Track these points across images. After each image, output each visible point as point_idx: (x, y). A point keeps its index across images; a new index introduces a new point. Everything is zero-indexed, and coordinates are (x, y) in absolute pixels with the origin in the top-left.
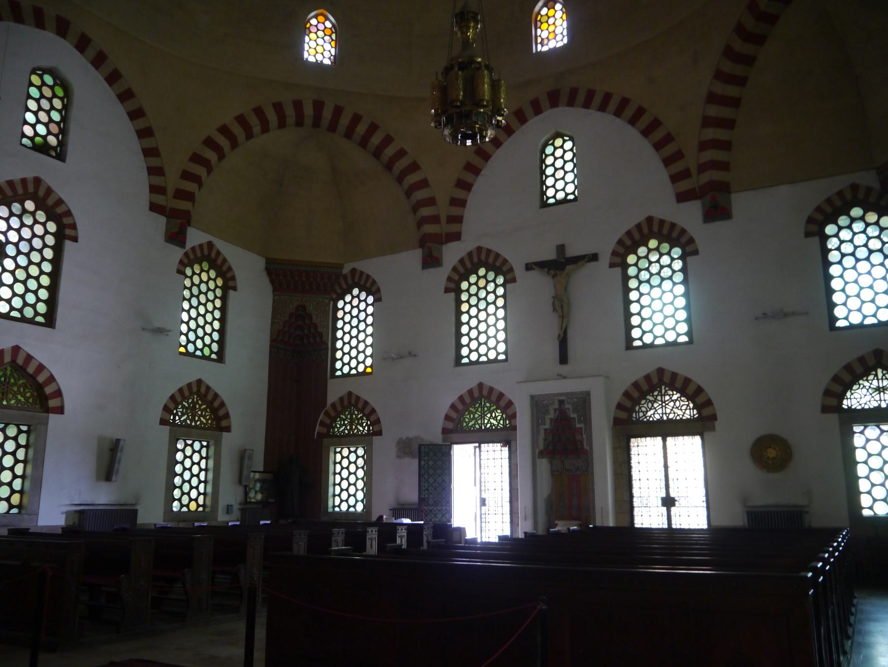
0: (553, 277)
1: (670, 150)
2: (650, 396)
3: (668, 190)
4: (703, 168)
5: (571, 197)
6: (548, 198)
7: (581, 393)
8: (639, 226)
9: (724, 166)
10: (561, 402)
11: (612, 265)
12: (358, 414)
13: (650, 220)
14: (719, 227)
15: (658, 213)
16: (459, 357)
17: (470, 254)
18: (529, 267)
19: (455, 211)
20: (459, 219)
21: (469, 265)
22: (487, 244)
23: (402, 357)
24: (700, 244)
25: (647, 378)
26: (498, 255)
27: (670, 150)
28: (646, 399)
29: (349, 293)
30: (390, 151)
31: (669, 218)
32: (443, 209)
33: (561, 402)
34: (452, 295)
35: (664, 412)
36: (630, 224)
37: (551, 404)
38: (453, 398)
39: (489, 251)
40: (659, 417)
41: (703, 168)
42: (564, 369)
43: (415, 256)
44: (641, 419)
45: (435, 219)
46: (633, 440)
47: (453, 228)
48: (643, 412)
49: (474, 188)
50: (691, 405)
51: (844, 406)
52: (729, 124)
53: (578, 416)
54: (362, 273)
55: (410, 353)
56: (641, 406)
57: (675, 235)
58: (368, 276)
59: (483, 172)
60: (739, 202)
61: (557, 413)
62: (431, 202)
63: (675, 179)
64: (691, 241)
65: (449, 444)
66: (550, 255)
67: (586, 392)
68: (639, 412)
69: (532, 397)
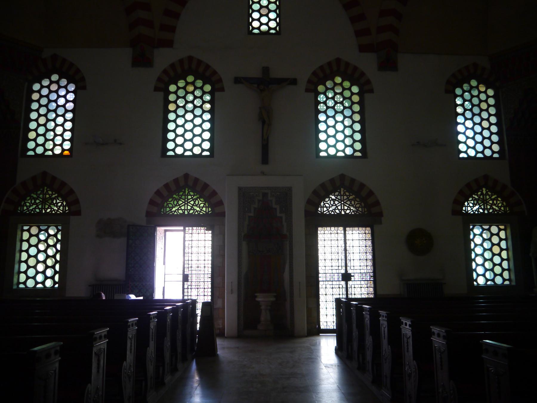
2: (332, 195)
6: (254, 28)
8: (329, 64)
10: (265, 195)
11: (307, 90)
12: (52, 194)
13: (338, 60)
17: (181, 61)
18: (237, 80)
20: (172, 29)
26: (208, 67)
28: (329, 198)
29: (47, 78)
33: (265, 195)
34: (161, 94)
38: (159, 185)
39: (200, 62)
44: (325, 213)
46: (320, 229)
48: (338, 209)
50: (363, 204)
63: (358, 34)
64: (368, 82)
65: (153, 226)
68: (323, 207)
69: (240, 189)
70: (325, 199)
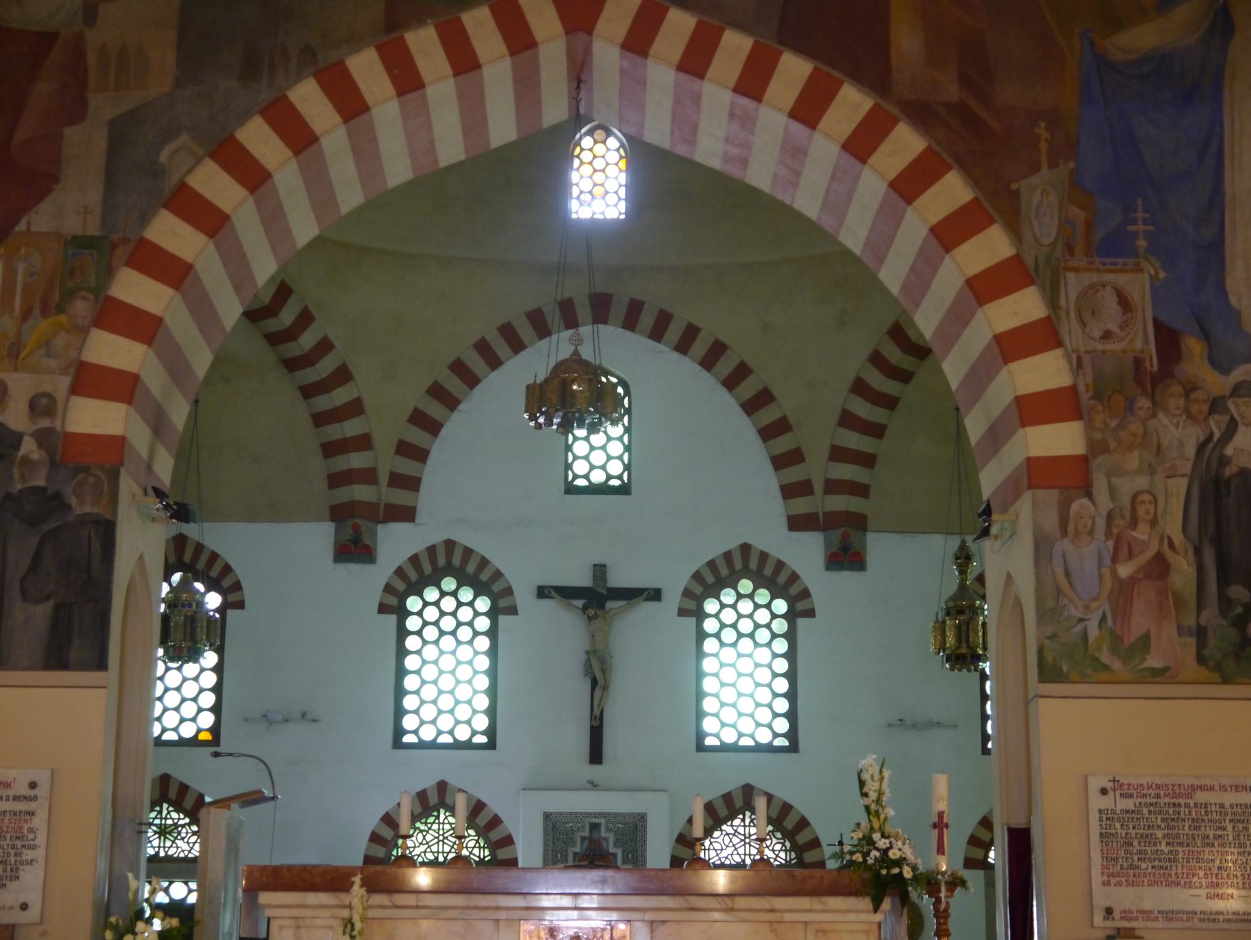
0: (590, 619)
1: (783, 443)
3: (775, 509)
4: (833, 487)
5: (615, 483)
6: (576, 477)
7: (629, 814)
8: (728, 556)
9: (861, 490)
11: (682, 612)
13: (745, 548)
14: (845, 579)
15: (759, 543)
16: (399, 732)
17: (431, 550)
18: (543, 592)
19: (406, 466)
20: (413, 484)
21: (427, 569)
22: (464, 538)
23: (287, 721)
25: (727, 798)
26: (484, 562)
27: (783, 443)
30: (308, 340)
31: (776, 552)
32: (385, 460)
33: (595, 827)
34: (392, 619)
35: (747, 853)
36: (715, 550)
37: (579, 829)
39: (468, 552)
40: (739, 860)
41: (833, 487)
42: (595, 772)
45: (369, 476)
47: (401, 497)
49: (444, 432)
50: (788, 844)
51: (990, 860)
52: (877, 431)
53: (623, 851)
54: (199, 547)
56: (712, 840)
57: (782, 579)
58: (214, 556)
59: (462, 407)
60: (878, 546)
61: (586, 843)
62: (363, 442)
63: (788, 492)
64: (806, 594)
66: (582, 579)
67: (639, 814)
69: (547, 816)
70: (713, 833)
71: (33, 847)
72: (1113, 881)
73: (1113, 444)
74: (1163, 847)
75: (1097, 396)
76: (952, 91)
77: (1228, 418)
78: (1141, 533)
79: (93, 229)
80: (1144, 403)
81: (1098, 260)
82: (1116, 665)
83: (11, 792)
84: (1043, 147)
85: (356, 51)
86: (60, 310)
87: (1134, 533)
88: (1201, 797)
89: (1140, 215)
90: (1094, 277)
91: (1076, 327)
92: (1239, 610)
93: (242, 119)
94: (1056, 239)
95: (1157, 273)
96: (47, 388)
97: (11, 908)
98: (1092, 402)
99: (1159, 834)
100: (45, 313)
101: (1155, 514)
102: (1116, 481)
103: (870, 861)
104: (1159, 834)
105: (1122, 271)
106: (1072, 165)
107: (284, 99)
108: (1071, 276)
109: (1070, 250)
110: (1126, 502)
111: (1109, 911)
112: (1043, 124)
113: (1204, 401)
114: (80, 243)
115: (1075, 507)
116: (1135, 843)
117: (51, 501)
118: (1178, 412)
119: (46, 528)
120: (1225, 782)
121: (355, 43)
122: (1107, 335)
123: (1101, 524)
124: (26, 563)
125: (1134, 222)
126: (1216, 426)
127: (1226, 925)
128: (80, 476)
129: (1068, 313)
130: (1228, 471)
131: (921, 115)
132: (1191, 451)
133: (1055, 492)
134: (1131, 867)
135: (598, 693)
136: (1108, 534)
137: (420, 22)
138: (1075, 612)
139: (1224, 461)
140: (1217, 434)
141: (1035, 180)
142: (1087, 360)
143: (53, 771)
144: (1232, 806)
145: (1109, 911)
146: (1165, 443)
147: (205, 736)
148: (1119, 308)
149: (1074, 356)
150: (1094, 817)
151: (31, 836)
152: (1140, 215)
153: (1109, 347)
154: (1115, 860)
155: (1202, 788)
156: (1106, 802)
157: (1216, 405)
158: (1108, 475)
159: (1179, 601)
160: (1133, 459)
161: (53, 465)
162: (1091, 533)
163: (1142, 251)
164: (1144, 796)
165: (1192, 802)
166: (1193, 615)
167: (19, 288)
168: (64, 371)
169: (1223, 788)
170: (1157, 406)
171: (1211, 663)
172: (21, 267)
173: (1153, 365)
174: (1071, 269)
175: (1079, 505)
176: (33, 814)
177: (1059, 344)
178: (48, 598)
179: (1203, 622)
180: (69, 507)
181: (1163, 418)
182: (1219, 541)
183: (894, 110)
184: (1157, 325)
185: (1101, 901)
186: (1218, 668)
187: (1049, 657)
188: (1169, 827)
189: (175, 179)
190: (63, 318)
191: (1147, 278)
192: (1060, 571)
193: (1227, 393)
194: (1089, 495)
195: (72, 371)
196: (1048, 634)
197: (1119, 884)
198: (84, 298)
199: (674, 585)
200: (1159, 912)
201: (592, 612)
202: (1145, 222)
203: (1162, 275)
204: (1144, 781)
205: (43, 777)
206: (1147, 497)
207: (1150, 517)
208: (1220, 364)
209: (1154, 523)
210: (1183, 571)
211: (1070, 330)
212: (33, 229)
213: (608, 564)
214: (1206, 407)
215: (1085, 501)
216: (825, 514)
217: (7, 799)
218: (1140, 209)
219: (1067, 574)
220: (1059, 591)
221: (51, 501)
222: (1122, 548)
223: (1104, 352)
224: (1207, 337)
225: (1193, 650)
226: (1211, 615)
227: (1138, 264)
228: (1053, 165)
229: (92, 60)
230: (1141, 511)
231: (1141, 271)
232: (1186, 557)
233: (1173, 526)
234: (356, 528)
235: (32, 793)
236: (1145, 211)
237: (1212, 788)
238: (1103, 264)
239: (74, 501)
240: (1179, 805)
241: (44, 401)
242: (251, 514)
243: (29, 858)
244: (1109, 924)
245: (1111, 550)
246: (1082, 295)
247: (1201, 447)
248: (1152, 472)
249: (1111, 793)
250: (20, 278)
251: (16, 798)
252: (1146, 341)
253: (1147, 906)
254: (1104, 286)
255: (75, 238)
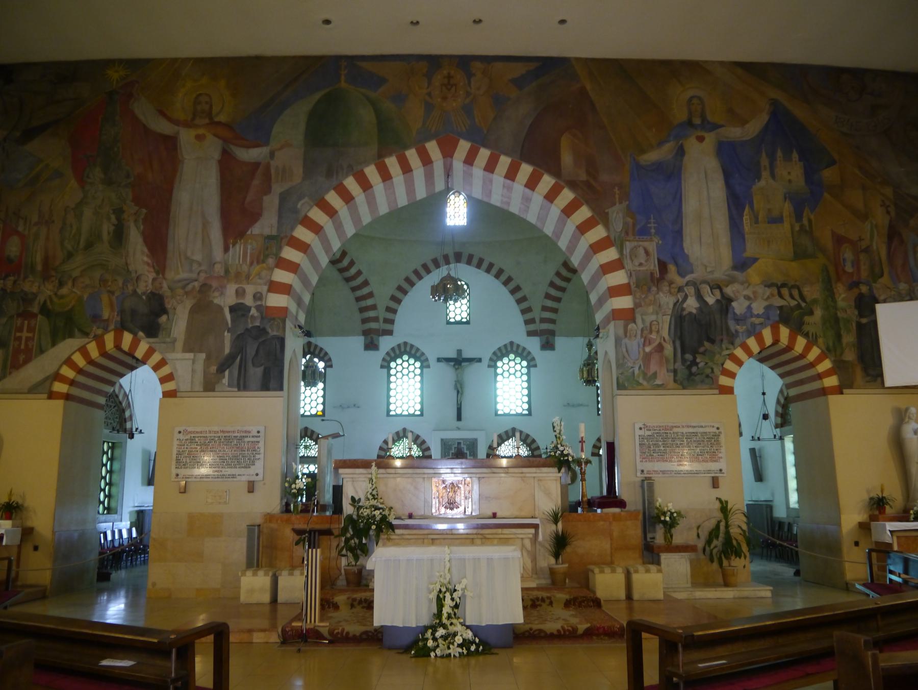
1: (525, 305)
3: (522, 329)
4: (543, 320)
5: (464, 320)
6: (450, 318)
8: (505, 346)
9: (553, 321)
10: (459, 443)
11: (489, 366)
13: (512, 343)
14: (548, 353)
15: (516, 341)
16: (389, 411)
17: (399, 346)
18: (439, 360)
19: (389, 316)
20: (392, 322)
21: (398, 352)
22: (411, 341)
24: (538, 361)
25: (506, 432)
26: (418, 350)
27: (525, 305)
30: (353, 271)
31: (523, 344)
32: (382, 313)
33: (459, 443)
34: (385, 370)
39: (412, 346)
41: (543, 320)
42: (459, 424)
43: (359, 341)
45: (376, 319)
47: (387, 327)
49: (402, 303)
50: (528, 449)
52: (558, 300)
54: (316, 346)
55: (355, 405)
58: (321, 349)
59: (409, 294)
60: (559, 341)
61: (456, 449)
62: (374, 307)
63: (527, 322)
64: (533, 359)
66: (453, 355)
67: (474, 439)
69: (442, 440)
71: (259, 454)
72: (644, 460)
73: (643, 304)
74: (662, 448)
75: (637, 286)
76: (583, 177)
77: (684, 294)
78: (654, 336)
79: (274, 233)
80: (654, 289)
81: (637, 237)
82: (645, 383)
83: (251, 435)
84: (617, 196)
85: (367, 166)
86: (263, 262)
87: (651, 336)
88: (675, 430)
89: (652, 220)
90: (636, 243)
91: (629, 261)
92: (689, 363)
93: (327, 191)
94: (622, 230)
95: (659, 241)
96: (259, 290)
97: (253, 475)
98: (636, 289)
99: (660, 443)
100: (258, 263)
101: (659, 329)
102: (644, 317)
103: (557, 455)
104: (660, 443)
105: (645, 241)
106: (627, 203)
107: (342, 184)
108: (627, 243)
109: (627, 233)
110: (648, 324)
111: (642, 471)
112: (617, 188)
113: (676, 288)
114: (270, 238)
115: (630, 327)
116: (652, 447)
117: (262, 331)
118: (666, 292)
119: (261, 340)
120: (684, 424)
121: (367, 164)
122: (641, 264)
123: (639, 332)
124: (253, 353)
125: (650, 223)
126: (680, 297)
127: (683, 475)
128: (272, 322)
129: (626, 257)
130: (685, 313)
131: (572, 185)
132: (671, 306)
133: (622, 321)
134: (650, 455)
135: (459, 395)
136: (642, 336)
137: (390, 155)
138: (630, 365)
139: (683, 309)
140: (680, 300)
141: (614, 208)
142: (633, 273)
143: (265, 427)
144: (686, 433)
145: (642, 471)
146: (662, 303)
147: (320, 413)
148: (645, 254)
149: (629, 272)
150: (637, 438)
151: (258, 450)
152: (652, 220)
153: (641, 269)
154: (645, 453)
155: (676, 427)
156: (642, 432)
157: (680, 289)
158: (642, 315)
159: (667, 361)
160: (651, 309)
161: (262, 318)
162: (635, 336)
163: (653, 234)
164: (655, 430)
165: (672, 432)
166: (673, 364)
167: (249, 254)
168: (265, 284)
169: (683, 427)
170: (659, 290)
171: (679, 382)
172: (249, 247)
173: (657, 275)
174: (628, 240)
175: (631, 326)
176: (259, 442)
177: (623, 268)
178: (261, 365)
179: (676, 367)
180: (268, 333)
181: (661, 294)
182: (682, 338)
183: (562, 184)
184: (659, 260)
185: (639, 468)
186: (681, 384)
187: (621, 381)
188: (664, 441)
189: (303, 214)
190: (264, 265)
191: (655, 244)
192: (624, 350)
193: (684, 285)
194: (635, 322)
195: (268, 284)
196: (620, 373)
197: (646, 461)
198: (272, 258)
199: (486, 357)
200: (660, 471)
201: (457, 367)
202: (654, 223)
203: (660, 242)
204: (655, 425)
205: (262, 429)
206: (655, 323)
207: (657, 330)
208: (682, 274)
209: (658, 332)
210: (669, 349)
211: (628, 263)
212: (253, 233)
213: (462, 349)
214: (676, 290)
215: (633, 325)
216: (540, 330)
217: (250, 437)
218: (652, 218)
219: (627, 351)
220: (624, 357)
221: (262, 331)
222: (647, 341)
223: (639, 270)
224: (676, 264)
225: (672, 378)
226: (679, 365)
227: (651, 238)
228: (621, 203)
229: (273, 171)
230: (653, 328)
231: (653, 241)
232: (670, 344)
233: (665, 333)
234: (372, 338)
235: (259, 435)
236: (654, 219)
237: (679, 427)
238: (639, 238)
239: (270, 331)
240: (668, 433)
241: (259, 295)
242: (334, 334)
243: (258, 457)
244: (642, 475)
245: (643, 342)
246: (632, 250)
247: (675, 304)
248: (657, 314)
249: (643, 429)
250: (249, 251)
251: (253, 437)
252: (655, 266)
253: (656, 469)
254: (639, 247)
255: (268, 236)
